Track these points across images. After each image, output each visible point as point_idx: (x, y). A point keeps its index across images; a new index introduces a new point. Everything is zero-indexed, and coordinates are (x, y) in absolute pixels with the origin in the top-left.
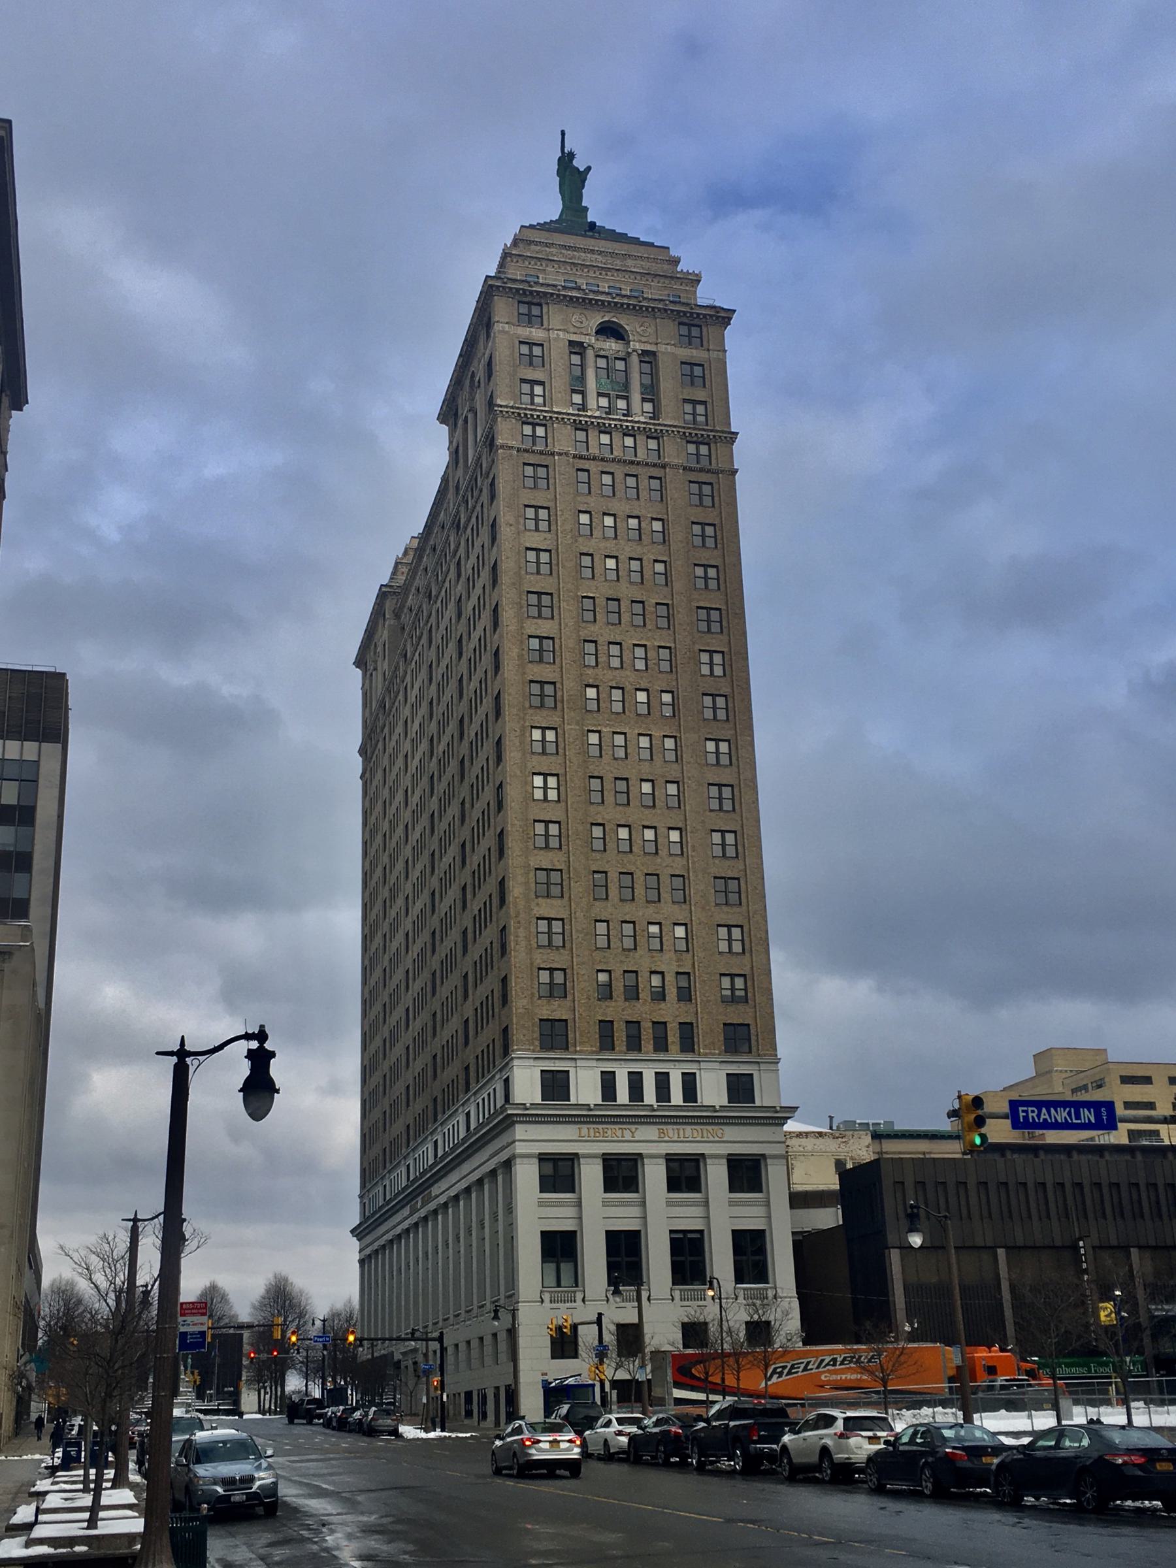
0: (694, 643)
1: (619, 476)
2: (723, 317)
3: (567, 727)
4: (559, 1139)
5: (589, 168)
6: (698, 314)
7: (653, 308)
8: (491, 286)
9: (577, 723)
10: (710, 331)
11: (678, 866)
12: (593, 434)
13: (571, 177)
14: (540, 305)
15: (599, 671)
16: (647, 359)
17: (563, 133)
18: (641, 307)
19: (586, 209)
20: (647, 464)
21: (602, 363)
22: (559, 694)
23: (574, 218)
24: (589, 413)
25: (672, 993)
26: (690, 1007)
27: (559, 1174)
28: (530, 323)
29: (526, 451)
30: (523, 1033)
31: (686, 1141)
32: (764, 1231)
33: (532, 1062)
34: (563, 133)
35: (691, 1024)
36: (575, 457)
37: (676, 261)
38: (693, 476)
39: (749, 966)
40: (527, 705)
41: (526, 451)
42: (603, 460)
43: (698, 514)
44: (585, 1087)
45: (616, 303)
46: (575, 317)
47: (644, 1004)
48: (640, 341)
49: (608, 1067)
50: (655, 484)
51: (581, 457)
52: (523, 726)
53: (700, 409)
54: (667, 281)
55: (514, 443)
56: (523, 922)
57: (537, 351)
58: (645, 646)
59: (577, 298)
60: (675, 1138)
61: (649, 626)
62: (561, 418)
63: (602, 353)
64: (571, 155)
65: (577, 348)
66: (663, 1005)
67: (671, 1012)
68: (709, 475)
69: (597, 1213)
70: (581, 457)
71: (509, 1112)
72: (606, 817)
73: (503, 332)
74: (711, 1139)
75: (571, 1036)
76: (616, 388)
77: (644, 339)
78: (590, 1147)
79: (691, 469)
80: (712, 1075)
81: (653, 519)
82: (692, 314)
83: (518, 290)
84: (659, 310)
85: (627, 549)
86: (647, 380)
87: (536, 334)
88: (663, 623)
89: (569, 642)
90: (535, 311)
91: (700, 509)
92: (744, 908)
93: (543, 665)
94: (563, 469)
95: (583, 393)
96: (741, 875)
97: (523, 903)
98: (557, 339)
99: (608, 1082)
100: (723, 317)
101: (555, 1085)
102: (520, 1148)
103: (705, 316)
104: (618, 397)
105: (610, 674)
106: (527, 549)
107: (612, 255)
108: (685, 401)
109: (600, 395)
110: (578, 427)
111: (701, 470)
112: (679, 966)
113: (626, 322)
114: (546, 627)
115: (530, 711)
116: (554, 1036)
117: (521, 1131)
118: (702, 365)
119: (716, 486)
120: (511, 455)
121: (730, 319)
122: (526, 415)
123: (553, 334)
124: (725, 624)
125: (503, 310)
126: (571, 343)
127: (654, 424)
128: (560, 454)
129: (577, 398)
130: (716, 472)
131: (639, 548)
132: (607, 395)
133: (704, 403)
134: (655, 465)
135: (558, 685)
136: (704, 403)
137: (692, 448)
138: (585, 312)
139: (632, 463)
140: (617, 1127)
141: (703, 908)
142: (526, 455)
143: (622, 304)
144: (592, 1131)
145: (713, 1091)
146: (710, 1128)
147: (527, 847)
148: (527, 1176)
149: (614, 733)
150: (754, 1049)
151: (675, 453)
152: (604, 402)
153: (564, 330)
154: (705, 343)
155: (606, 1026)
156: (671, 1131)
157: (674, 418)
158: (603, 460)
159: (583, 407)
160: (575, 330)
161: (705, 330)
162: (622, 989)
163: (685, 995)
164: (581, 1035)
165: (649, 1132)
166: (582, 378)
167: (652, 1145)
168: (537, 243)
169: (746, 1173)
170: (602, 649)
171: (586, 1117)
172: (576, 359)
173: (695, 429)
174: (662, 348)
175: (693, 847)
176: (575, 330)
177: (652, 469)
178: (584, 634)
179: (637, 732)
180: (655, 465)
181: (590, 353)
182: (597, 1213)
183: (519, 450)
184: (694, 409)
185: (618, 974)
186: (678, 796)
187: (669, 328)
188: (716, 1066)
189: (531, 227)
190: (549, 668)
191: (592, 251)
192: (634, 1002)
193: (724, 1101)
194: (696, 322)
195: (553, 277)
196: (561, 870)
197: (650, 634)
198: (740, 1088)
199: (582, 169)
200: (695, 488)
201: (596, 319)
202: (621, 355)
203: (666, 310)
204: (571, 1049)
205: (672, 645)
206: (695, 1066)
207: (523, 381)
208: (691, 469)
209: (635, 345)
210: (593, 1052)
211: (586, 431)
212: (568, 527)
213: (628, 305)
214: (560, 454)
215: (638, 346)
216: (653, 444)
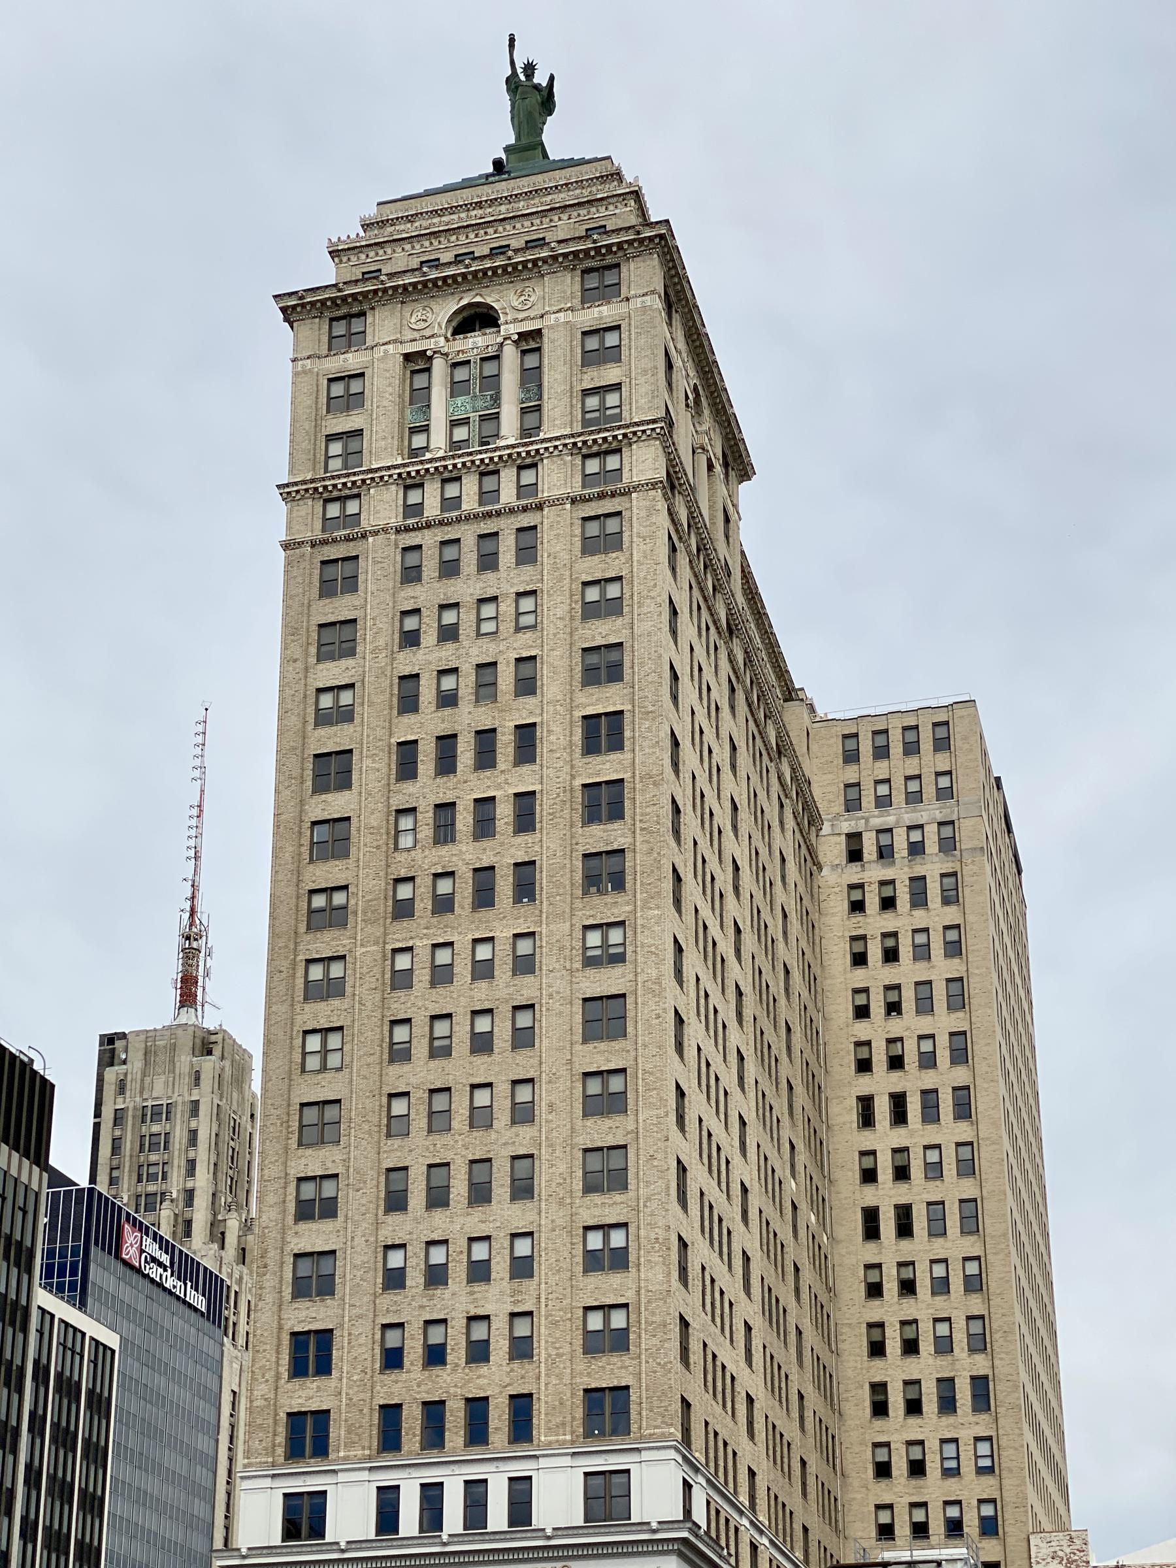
0: (573, 777)
11: (522, 1139)
23: (527, 148)
29: (324, 542)
36: (398, 531)
46: (418, 315)
51: (407, 529)
63: (461, 358)
65: (417, 363)
85: (474, 651)
109: (454, 424)
113: (497, 298)
123: (380, 352)
126: (407, 357)
128: (376, 533)
139: (488, 515)
142: (326, 549)
153: (395, 341)
158: (441, 523)
160: (416, 335)
175: (551, 1105)
176: (416, 335)
179: (470, 937)
181: (438, 365)
201: (446, 309)
214: (376, 533)
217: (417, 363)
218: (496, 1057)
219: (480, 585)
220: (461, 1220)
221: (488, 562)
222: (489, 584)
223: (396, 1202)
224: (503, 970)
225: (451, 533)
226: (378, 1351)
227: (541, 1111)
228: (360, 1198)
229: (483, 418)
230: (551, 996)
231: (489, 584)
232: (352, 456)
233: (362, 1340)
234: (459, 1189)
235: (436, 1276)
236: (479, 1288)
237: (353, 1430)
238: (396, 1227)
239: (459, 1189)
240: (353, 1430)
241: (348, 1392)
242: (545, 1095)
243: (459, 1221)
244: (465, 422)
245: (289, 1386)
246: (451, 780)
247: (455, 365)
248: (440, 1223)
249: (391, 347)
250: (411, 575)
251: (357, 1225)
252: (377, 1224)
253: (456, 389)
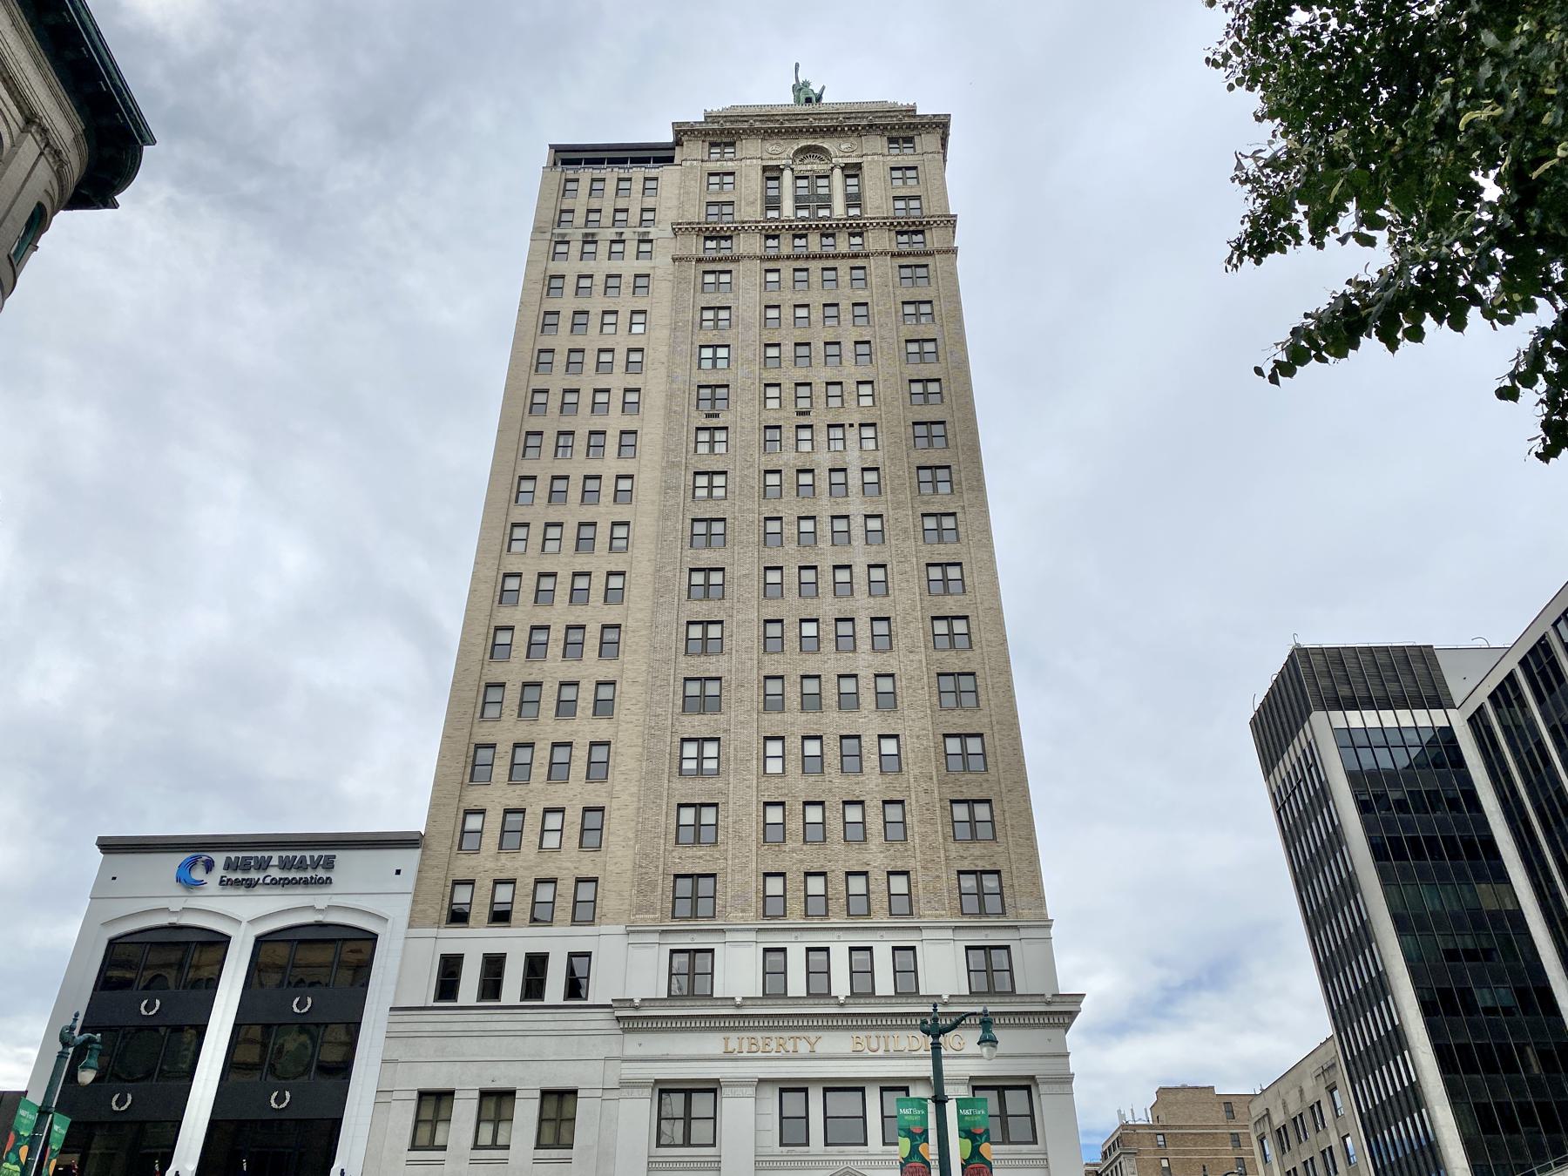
44: (737, 972)
49: (775, 941)
79: (900, 255)
104: (820, 207)
126: (765, 169)
133: (918, 198)
140: (786, 1035)
144: (745, 1042)
151: (878, 240)
171: (736, 1020)
180: (855, 256)
181: (787, 174)
187: (877, 143)
208: (900, 255)
217: (772, 173)
247: (798, 178)
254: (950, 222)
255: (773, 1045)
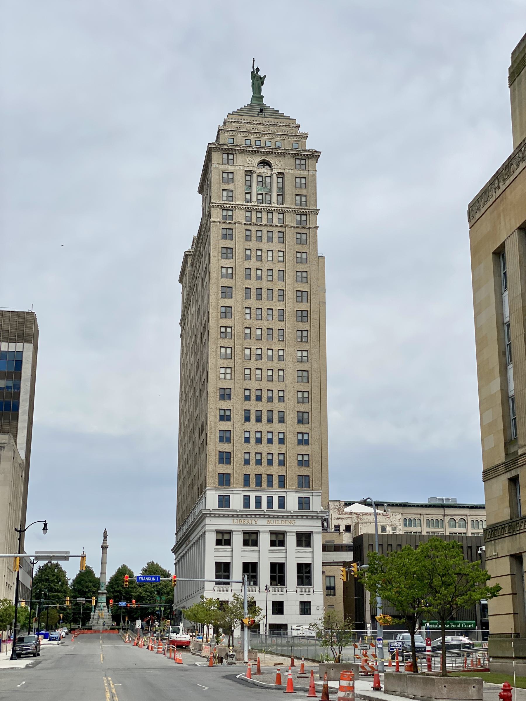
1: (265, 232)
2: (315, 155)
3: (236, 346)
4: (225, 524)
5: (265, 76)
6: (304, 155)
7: (284, 153)
8: (211, 148)
9: (240, 345)
10: (310, 162)
11: (281, 407)
12: (254, 213)
13: (258, 81)
14: (232, 154)
15: (251, 321)
16: (280, 176)
17: (254, 60)
18: (278, 153)
19: (263, 97)
20: (277, 226)
21: (260, 179)
22: (233, 332)
24: (252, 204)
25: (276, 462)
26: (284, 468)
27: (224, 539)
28: (228, 163)
30: (212, 480)
31: (278, 526)
32: (311, 564)
33: (214, 492)
34: (254, 60)
35: (284, 475)
36: (245, 224)
37: (298, 127)
38: (298, 231)
39: (311, 450)
40: (219, 337)
41: (223, 223)
42: (257, 225)
43: (299, 248)
44: (237, 502)
45: (267, 152)
47: (264, 467)
48: (277, 168)
49: (247, 494)
50: (281, 235)
51: (248, 224)
52: (217, 347)
53: (303, 199)
54: (292, 137)
55: (218, 220)
56: (213, 432)
57: (230, 176)
58: (272, 309)
59: (249, 151)
60: (274, 524)
61: (274, 300)
62: (239, 207)
63: (260, 174)
64: (258, 70)
65: (249, 173)
66: (272, 467)
67: (275, 470)
68: (306, 229)
69: (238, 555)
70: (248, 224)
71: (203, 513)
72: (251, 386)
73: (216, 168)
74: (289, 524)
75: (231, 480)
76: (266, 190)
77: (279, 167)
78: (237, 528)
80: (292, 497)
81: (279, 251)
82: (301, 155)
83: (222, 148)
84: (286, 153)
85: (267, 265)
86: (280, 186)
87: (230, 168)
88: (281, 298)
89: (238, 309)
90: (231, 157)
91: (300, 246)
92: (310, 425)
93: (227, 319)
94: (239, 232)
95: (250, 194)
96: (309, 411)
97: (213, 424)
98: (240, 170)
99: (247, 500)
100: (315, 155)
101: (224, 501)
102: (207, 528)
103: (307, 155)
104: (266, 194)
105: (256, 322)
106: (222, 267)
107: (269, 125)
108: (297, 195)
109: (258, 194)
110: (247, 210)
111: (302, 228)
112: (280, 451)
114: (228, 302)
115: (221, 340)
116: (224, 480)
117: (208, 521)
118: (305, 178)
119: (308, 235)
120: (217, 225)
121: (319, 156)
122: (224, 206)
123: (238, 168)
124: (309, 298)
125: (216, 157)
127: (282, 208)
128: (238, 223)
129: (248, 196)
130: (309, 228)
131: (271, 265)
132: (262, 194)
134: (281, 226)
135: (233, 328)
136: (305, 196)
137: (298, 217)
138: (253, 156)
139: (271, 226)
140: (249, 519)
141: (292, 425)
143: (269, 152)
145: (292, 503)
146: (289, 520)
147: (216, 400)
148: (211, 539)
149: (257, 349)
150: (311, 486)
152: (260, 197)
154: (307, 167)
155: (247, 477)
156: (272, 521)
157: (290, 204)
158: (257, 225)
159: (250, 201)
160: (248, 165)
161: (307, 162)
162: (255, 460)
163: (282, 463)
164: (236, 480)
165: (264, 521)
166: (251, 186)
167: (264, 527)
168: (234, 122)
169: (304, 539)
170: (254, 311)
171: (236, 515)
172: (248, 178)
173: (300, 209)
174: (287, 171)
176: (248, 165)
177: (279, 228)
178: (245, 305)
180: (281, 226)
181: (255, 176)
182: (238, 555)
183: (220, 222)
184: (301, 199)
185: (253, 454)
186: (284, 376)
187: (290, 161)
188: (294, 494)
189: (234, 114)
190: (230, 320)
191: (260, 124)
192: (259, 466)
193: (296, 509)
194: (303, 158)
195: (240, 140)
196: (230, 410)
197: (274, 304)
198: (304, 503)
199: (262, 76)
200: (299, 236)
201: (258, 159)
202: (269, 175)
203: (289, 154)
204: (231, 486)
205: (284, 309)
206: (285, 494)
207: (224, 190)
208: (298, 228)
209: (275, 171)
210: (240, 488)
211: (251, 212)
212: (240, 257)
213: (272, 152)
214: (238, 223)
215: (275, 171)
216: (281, 216)
217: (249, 173)
218: (274, 383)
219: (268, 246)
220: (265, 426)
221: (270, 239)
222: (271, 246)
223: (247, 419)
224: (276, 359)
225: (260, 228)
226: (243, 459)
227: (286, 399)
228: (238, 417)
229: (266, 194)
230: (289, 368)
231: (271, 246)
232: (230, 198)
233: (239, 456)
234: (264, 418)
235: (259, 441)
236: (270, 445)
237: (237, 479)
238: (247, 426)
239: (264, 418)
240: (237, 479)
241: (236, 469)
242: (288, 396)
243: (264, 426)
244: (262, 194)
245: (219, 466)
246: (261, 302)
248: (259, 426)
249: (241, 167)
250: (248, 238)
251: (237, 424)
252: (242, 425)
253: (261, 184)
254: (316, 212)
255: (246, 521)
